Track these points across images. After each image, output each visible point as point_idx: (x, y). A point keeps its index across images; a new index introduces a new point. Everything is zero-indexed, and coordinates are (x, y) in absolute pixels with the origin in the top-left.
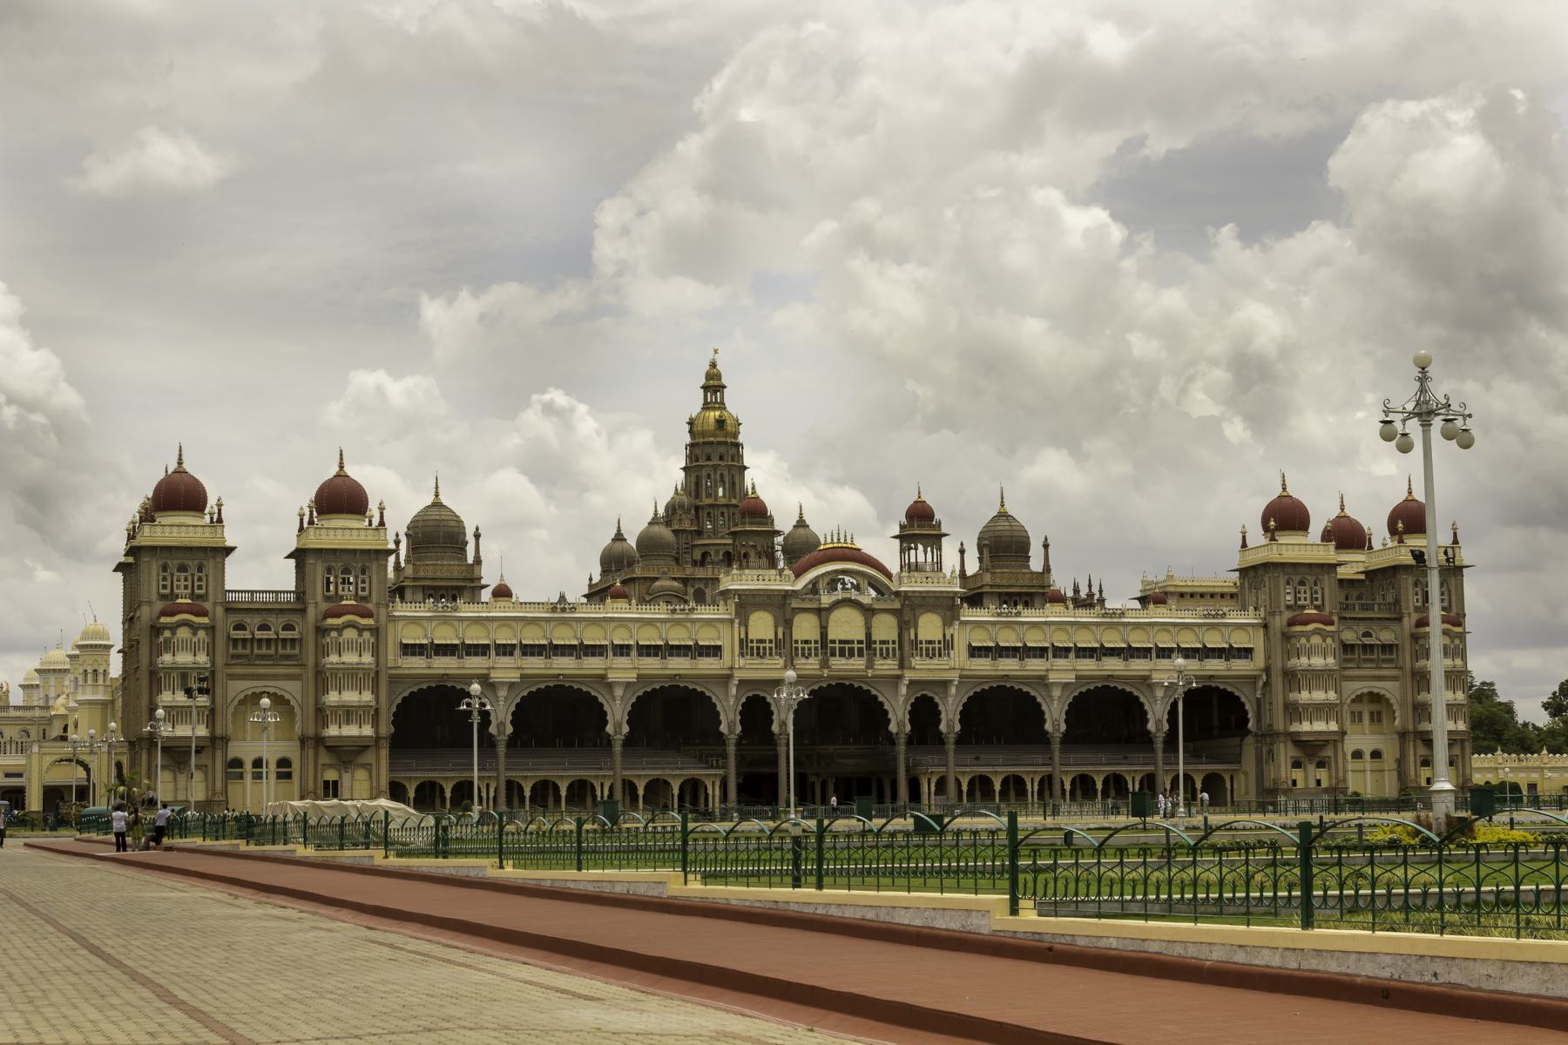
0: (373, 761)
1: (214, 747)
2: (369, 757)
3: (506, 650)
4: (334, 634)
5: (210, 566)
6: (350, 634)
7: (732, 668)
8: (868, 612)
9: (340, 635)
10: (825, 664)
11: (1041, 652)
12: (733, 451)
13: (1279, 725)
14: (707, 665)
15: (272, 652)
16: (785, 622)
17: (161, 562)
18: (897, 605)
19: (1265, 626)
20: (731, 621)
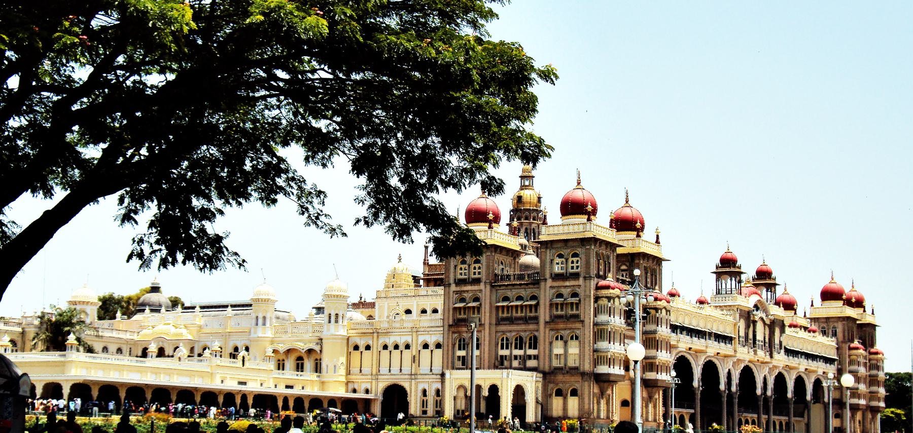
10: (755, 352)
16: (747, 327)
18: (768, 322)
19: (837, 349)
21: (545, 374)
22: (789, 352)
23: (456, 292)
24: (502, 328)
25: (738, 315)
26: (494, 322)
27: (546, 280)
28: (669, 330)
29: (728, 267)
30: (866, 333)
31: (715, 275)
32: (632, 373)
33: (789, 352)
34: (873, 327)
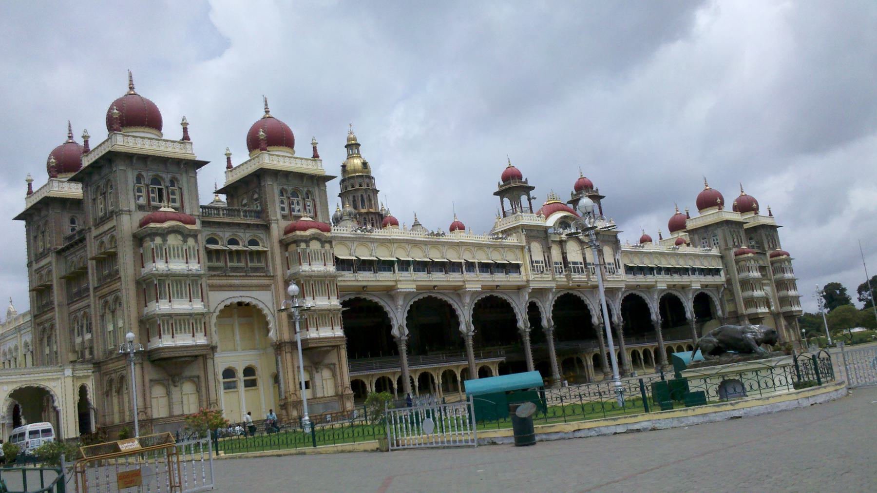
0: (335, 361)
1: (204, 357)
2: (332, 358)
3: (404, 265)
4: (303, 245)
5: (183, 180)
6: (315, 245)
7: (528, 281)
8: (581, 242)
9: (308, 246)
11: (650, 270)
12: (367, 180)
13: (743, 310)
14: (513, 279)
15: (242, 264)
16: (547, 249)
17: (136, 173)
19: (722, 257)
20: (522, 248)
21: (98, 365)
22: (630, 270)
23: (38, 271)
24: (74, 307)
25: (523, 237)
26: (65, 302)
27: (90, 229)
28: (331, 268)
29: (513, 186)
30: (764, 235)
31: (498, 197)
32: (271, 334)
33: (630, 270)
34: (774, 228)
